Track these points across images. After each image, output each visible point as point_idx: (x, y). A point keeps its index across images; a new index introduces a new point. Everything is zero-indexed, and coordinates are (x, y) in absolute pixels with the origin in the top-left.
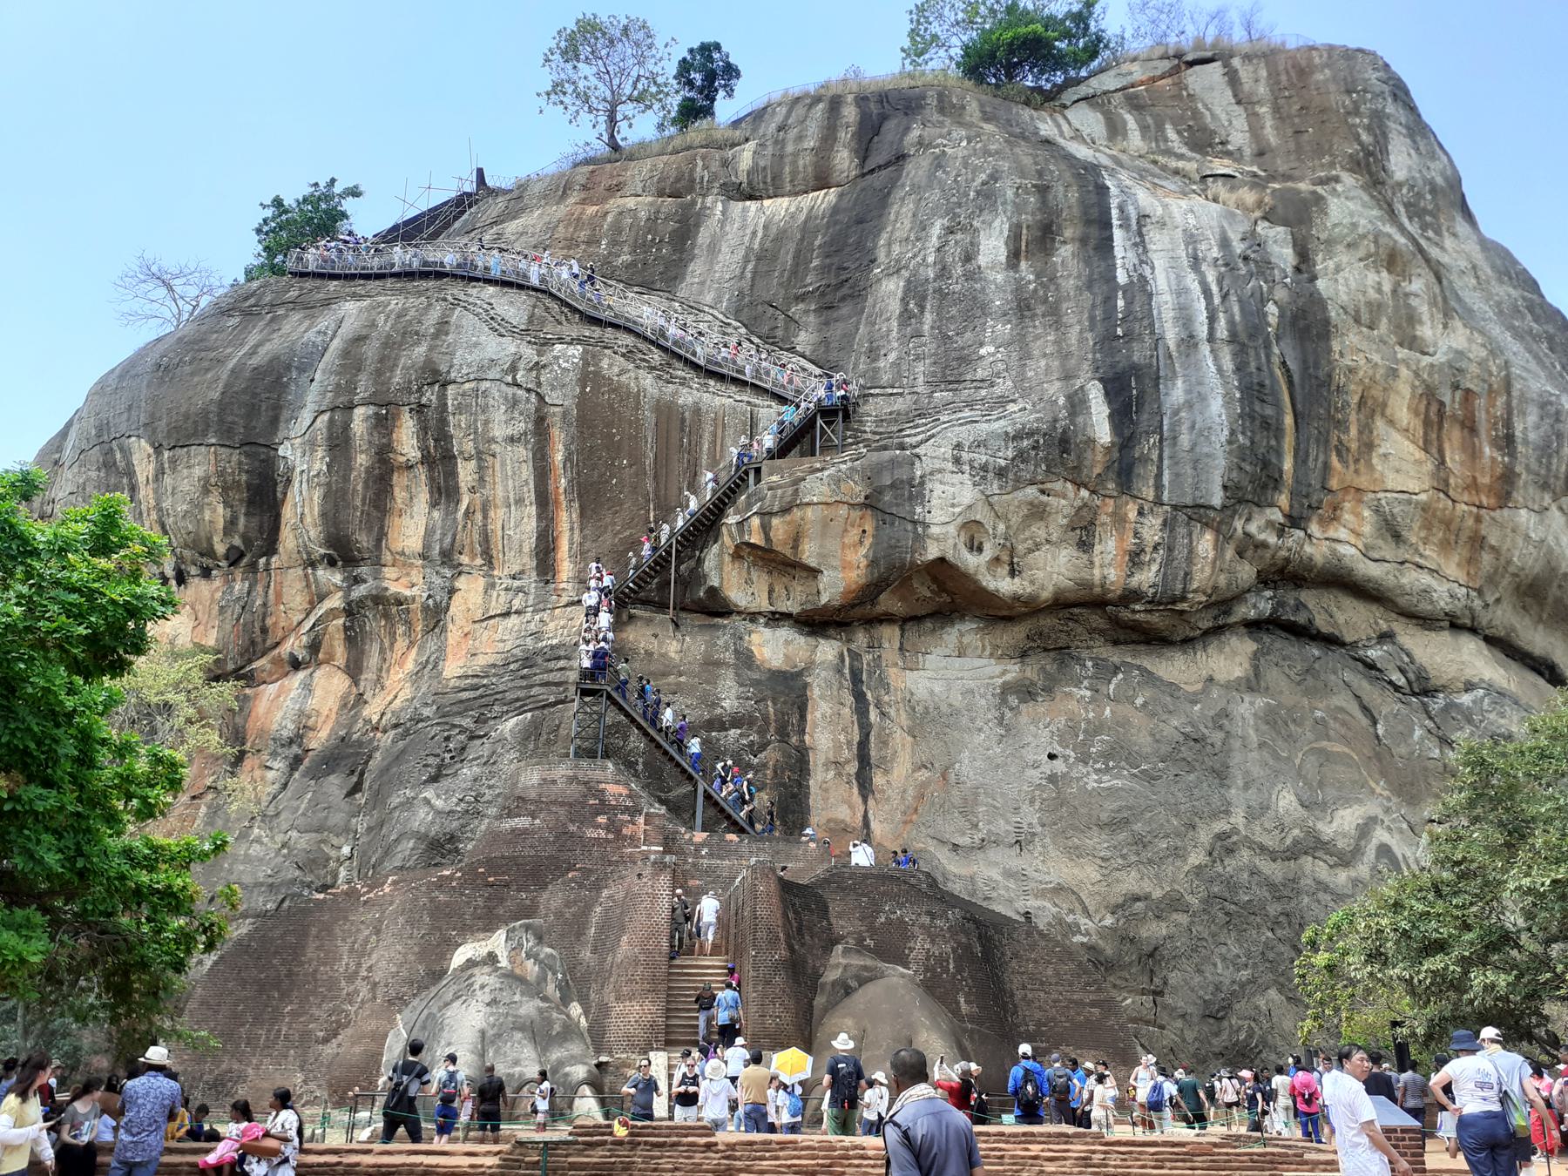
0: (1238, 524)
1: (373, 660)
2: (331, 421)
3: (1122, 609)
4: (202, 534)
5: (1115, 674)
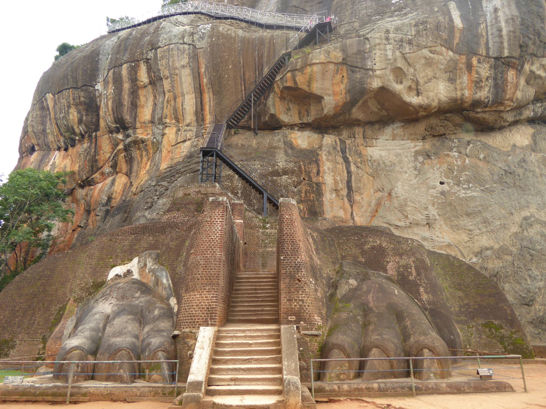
0: (527, 67)
1: (135, 168)
2: (114, 71)
3: (471, 112)
5: (469, 145)
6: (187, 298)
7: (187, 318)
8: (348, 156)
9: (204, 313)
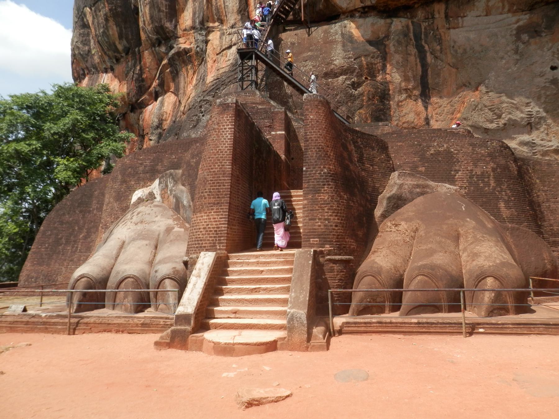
1: (182, 85)
4: (111, 42)
6: (195, 221)
7: (194, 243)
8: (423, 43)
9: (211, 237)
